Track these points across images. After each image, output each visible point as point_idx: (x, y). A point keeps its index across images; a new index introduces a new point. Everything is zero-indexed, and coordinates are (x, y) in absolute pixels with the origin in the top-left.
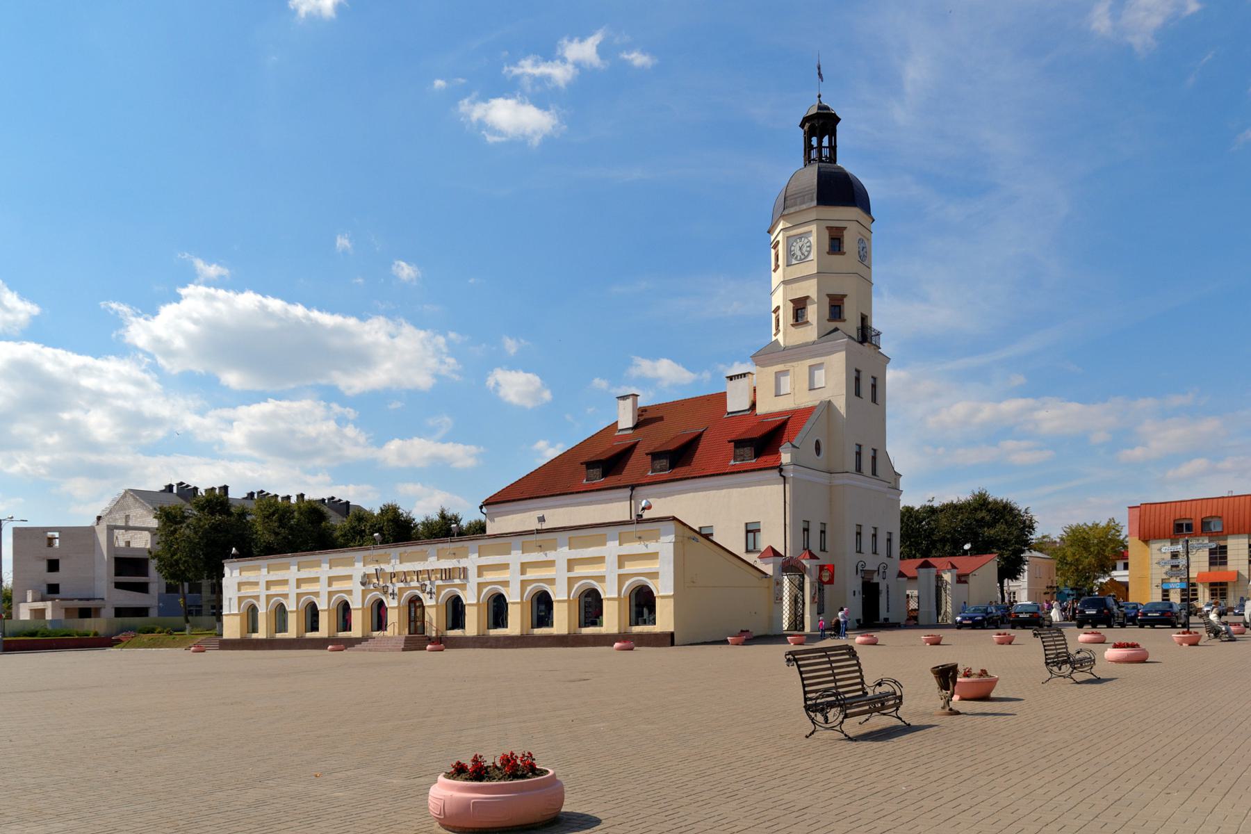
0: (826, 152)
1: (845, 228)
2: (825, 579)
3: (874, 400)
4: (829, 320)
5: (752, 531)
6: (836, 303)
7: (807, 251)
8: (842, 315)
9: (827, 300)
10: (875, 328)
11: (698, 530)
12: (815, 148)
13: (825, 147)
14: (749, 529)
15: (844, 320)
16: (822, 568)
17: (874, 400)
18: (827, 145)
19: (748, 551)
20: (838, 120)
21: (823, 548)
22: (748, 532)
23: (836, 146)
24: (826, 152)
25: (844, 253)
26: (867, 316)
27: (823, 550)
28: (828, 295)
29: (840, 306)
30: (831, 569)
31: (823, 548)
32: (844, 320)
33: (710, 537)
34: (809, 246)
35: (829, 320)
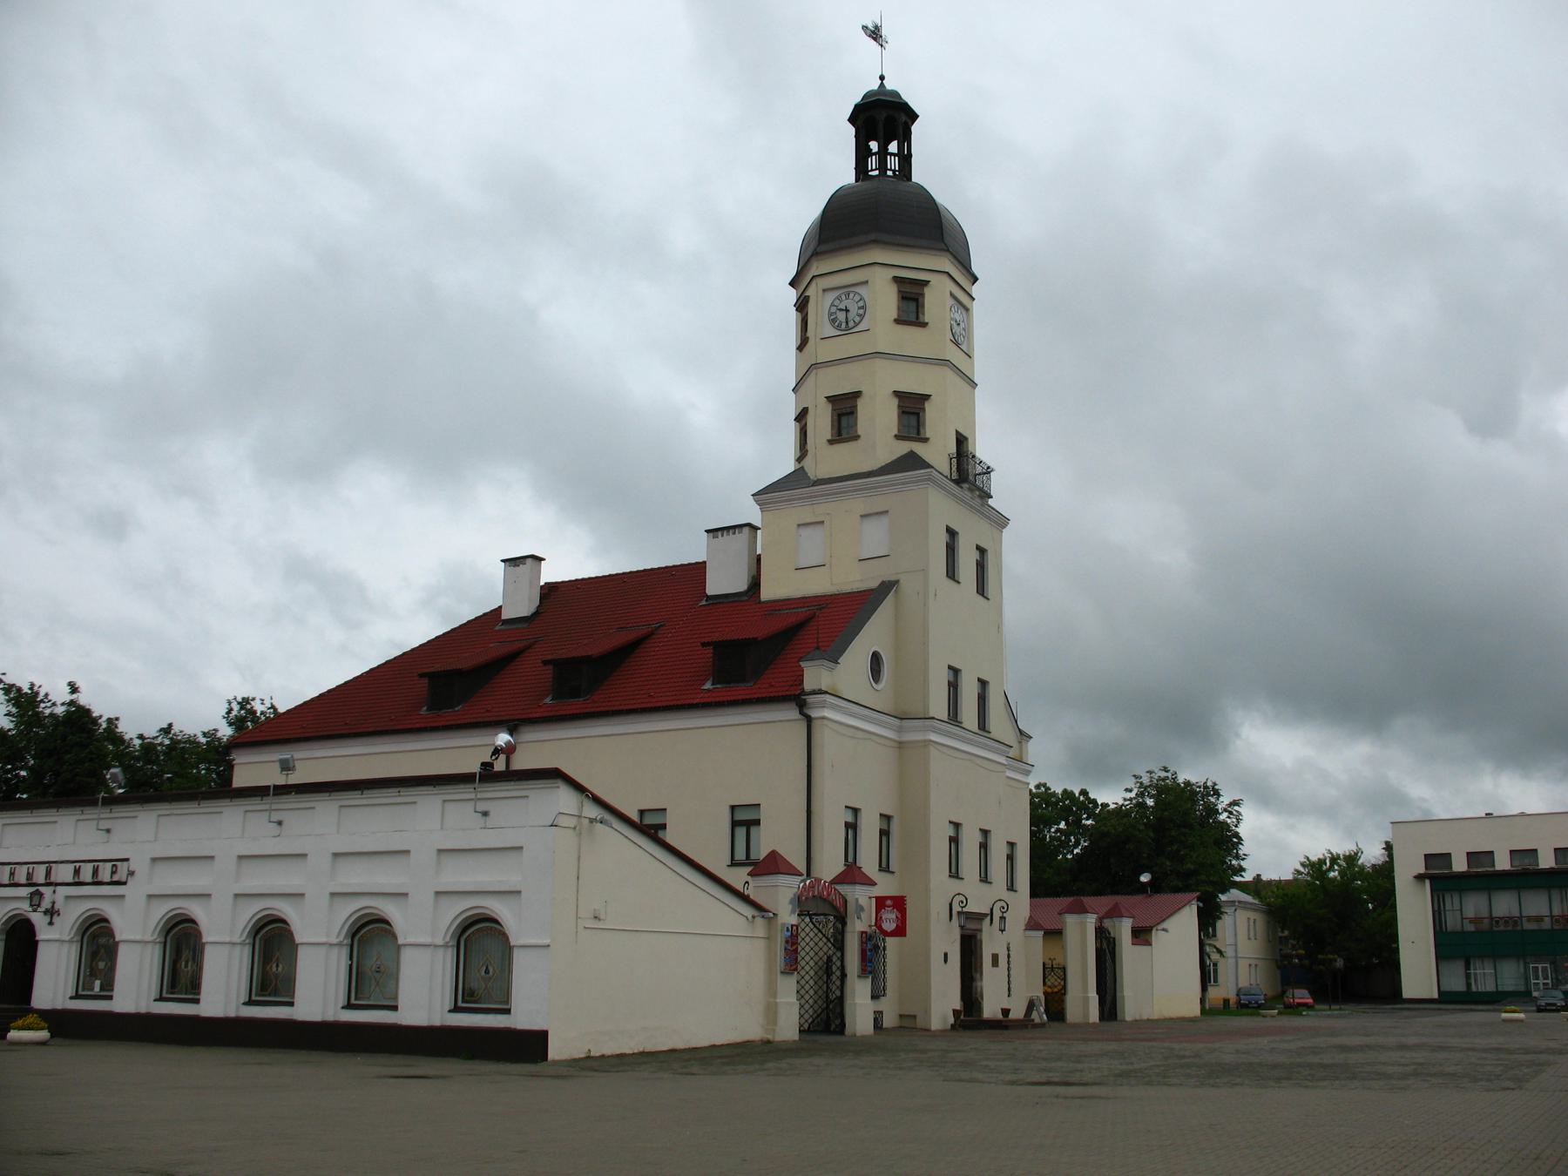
0: (893, 163)
1: (926, 283)
2: (889, 926)
3: (981, 589)
4: (897, 437)
5: (744, 821)
7: (859, 315)
8: (922, 430)
9: (895, 402)
10: (982, 459)
11: (635, 817)
12: (875, 154)
13: (891, 154)
14: (736, 818)
16: (881, 902)
17: (981, 589)
18: (896, 151)
19: (734, 863)
20: (913, 116)
21: (884, 865)
22: (735, 824)
23: (910, 155)
24: (893, 163)
25: (924, 325)
26: (966, 439)
27: (885, 868)
29: (918, 414)
30: (899, 903)
31: (884, 865)
32: (926, 440)
33: (661, 834)
34: (862, 308)
35: (897, 437)
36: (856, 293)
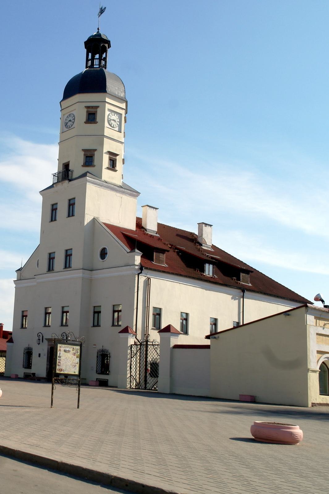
1: (97, 107)
4: (83, 166)
6: (89, 154)
9: (82, 153)
13: (97, 59)
15: (94, 166)
18: (98, 58)
28: (83, 150)
32: (94, 166)
35: (83, 166)
36: (73, 114)
